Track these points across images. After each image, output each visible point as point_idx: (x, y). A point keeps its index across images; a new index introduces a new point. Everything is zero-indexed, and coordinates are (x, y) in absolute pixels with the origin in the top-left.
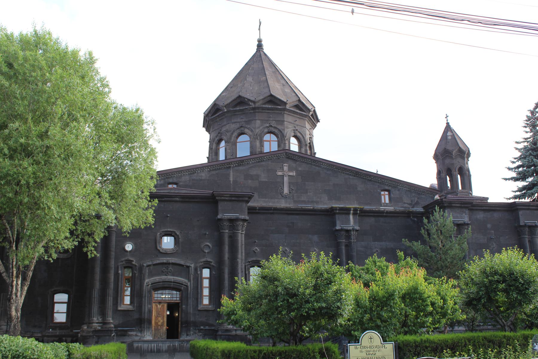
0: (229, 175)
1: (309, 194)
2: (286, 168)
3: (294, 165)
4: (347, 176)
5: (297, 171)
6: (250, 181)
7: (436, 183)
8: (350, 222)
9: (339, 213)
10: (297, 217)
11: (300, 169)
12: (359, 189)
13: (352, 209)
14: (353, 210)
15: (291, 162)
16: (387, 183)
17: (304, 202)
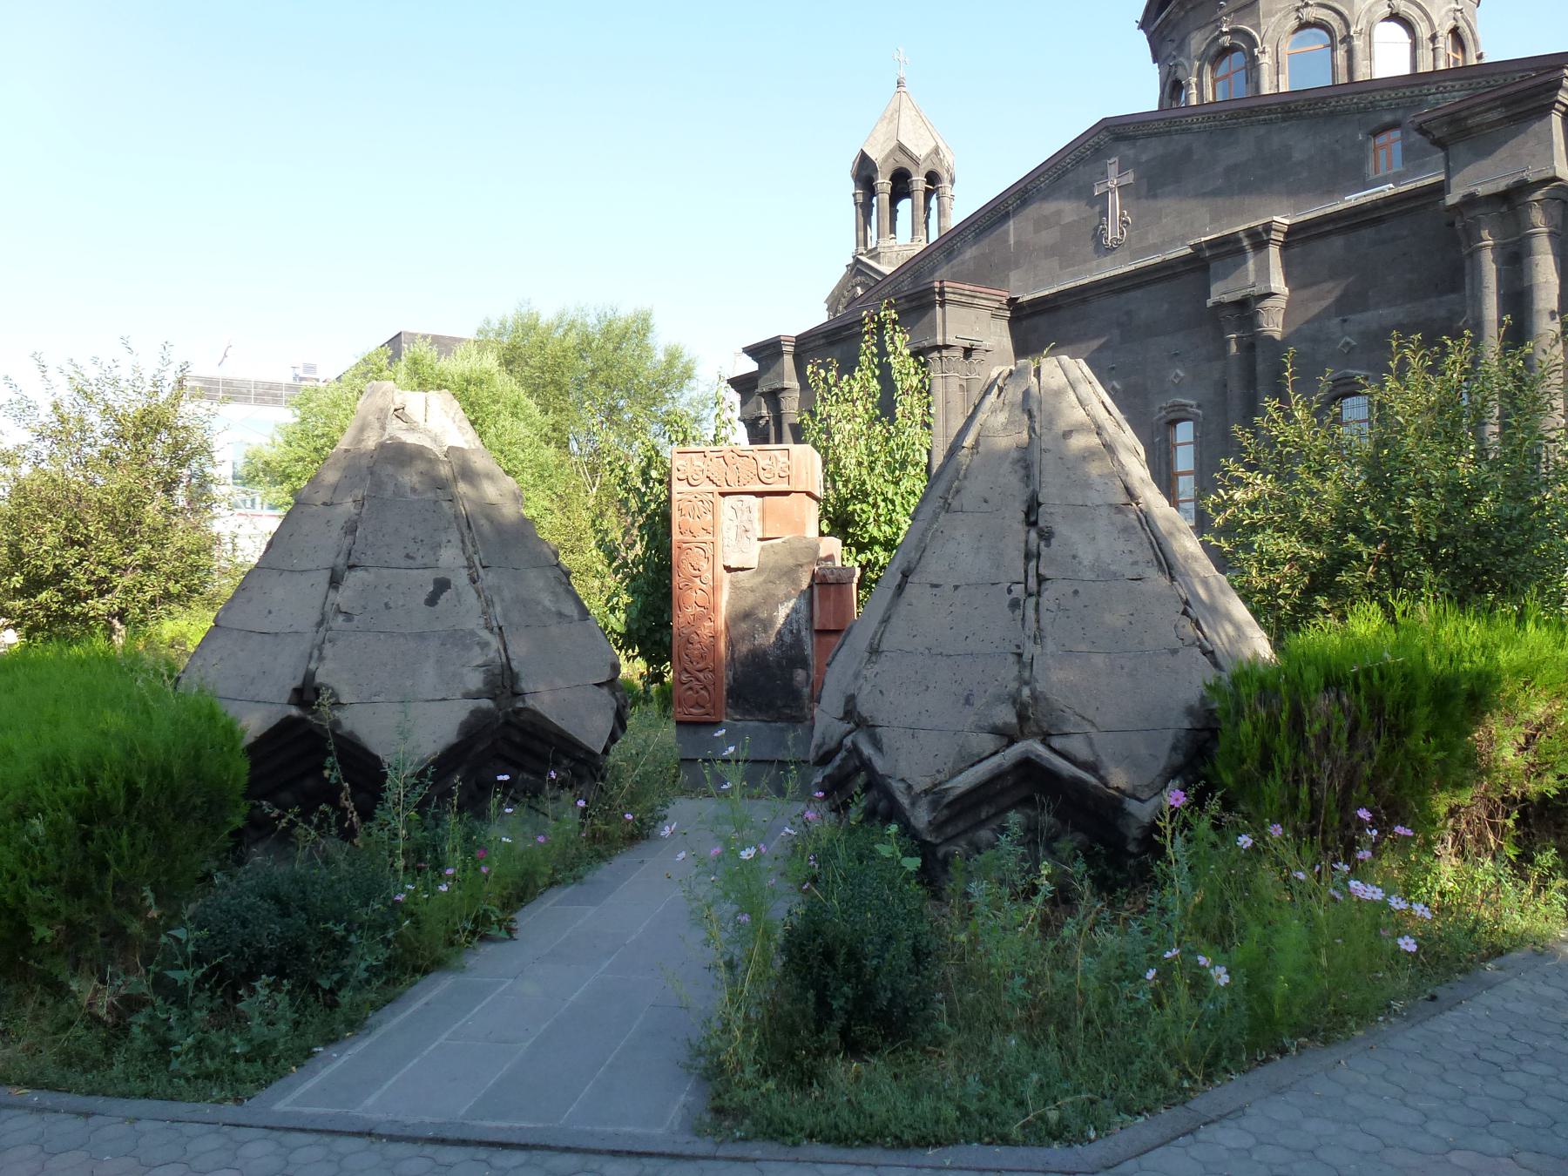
0: (1007, 232)
1: (1164, 221)
2: (1113, 169)
3: (1131, 153)
4: (1262, 130)
5: (1136, 165)
6: (1044, 233)
7: (1379, 73)
8: (1247, 275)
9: (1214, 257)
10: (1138, 293)
11: (1144, 158)
12: (1297, 156)
13: (1242, 235)
14: (1247, 236)
15: (1127, 150)
16: (1384, 104)
17: (1156, 249)
